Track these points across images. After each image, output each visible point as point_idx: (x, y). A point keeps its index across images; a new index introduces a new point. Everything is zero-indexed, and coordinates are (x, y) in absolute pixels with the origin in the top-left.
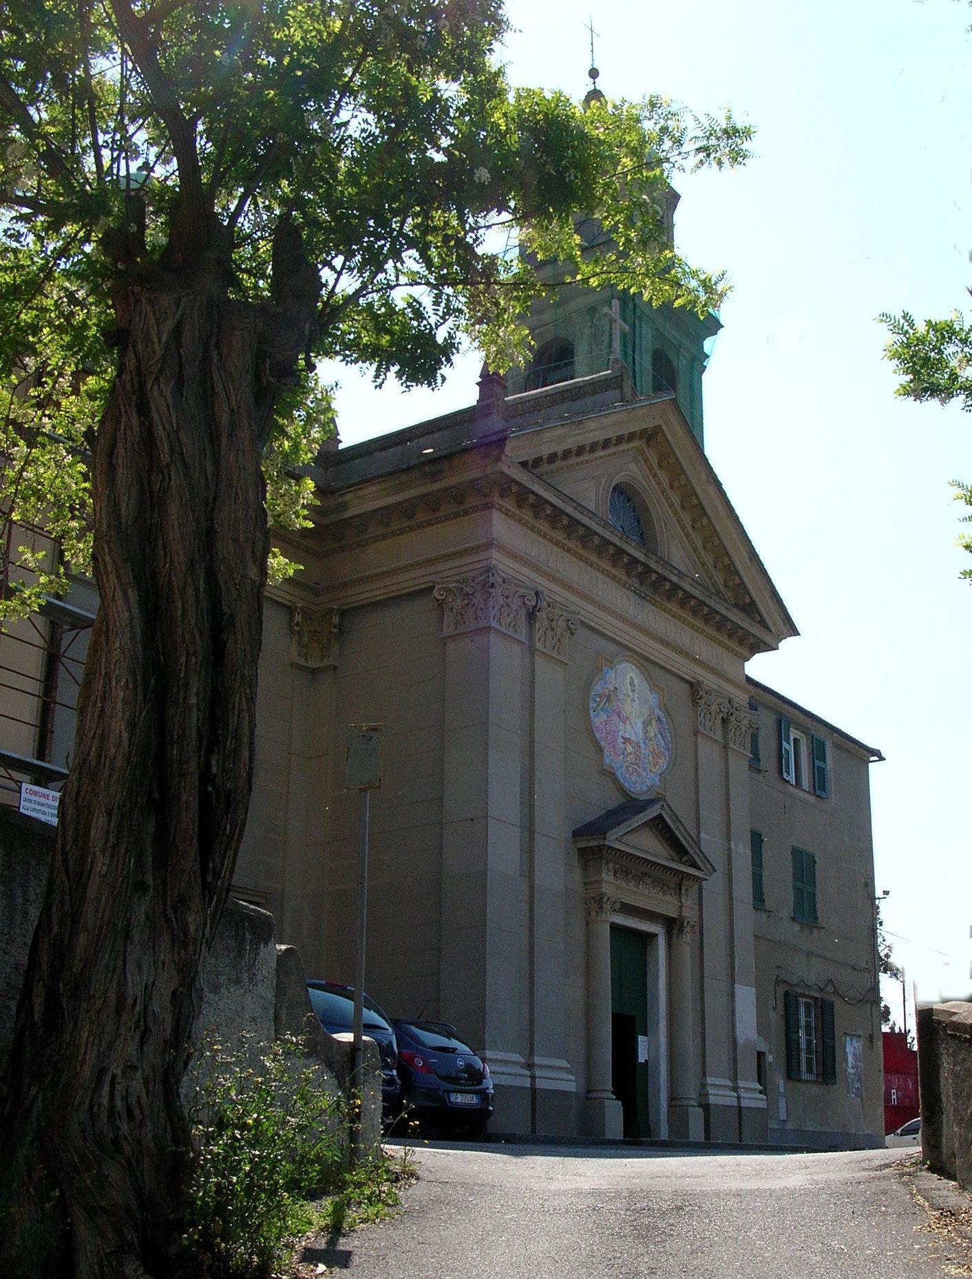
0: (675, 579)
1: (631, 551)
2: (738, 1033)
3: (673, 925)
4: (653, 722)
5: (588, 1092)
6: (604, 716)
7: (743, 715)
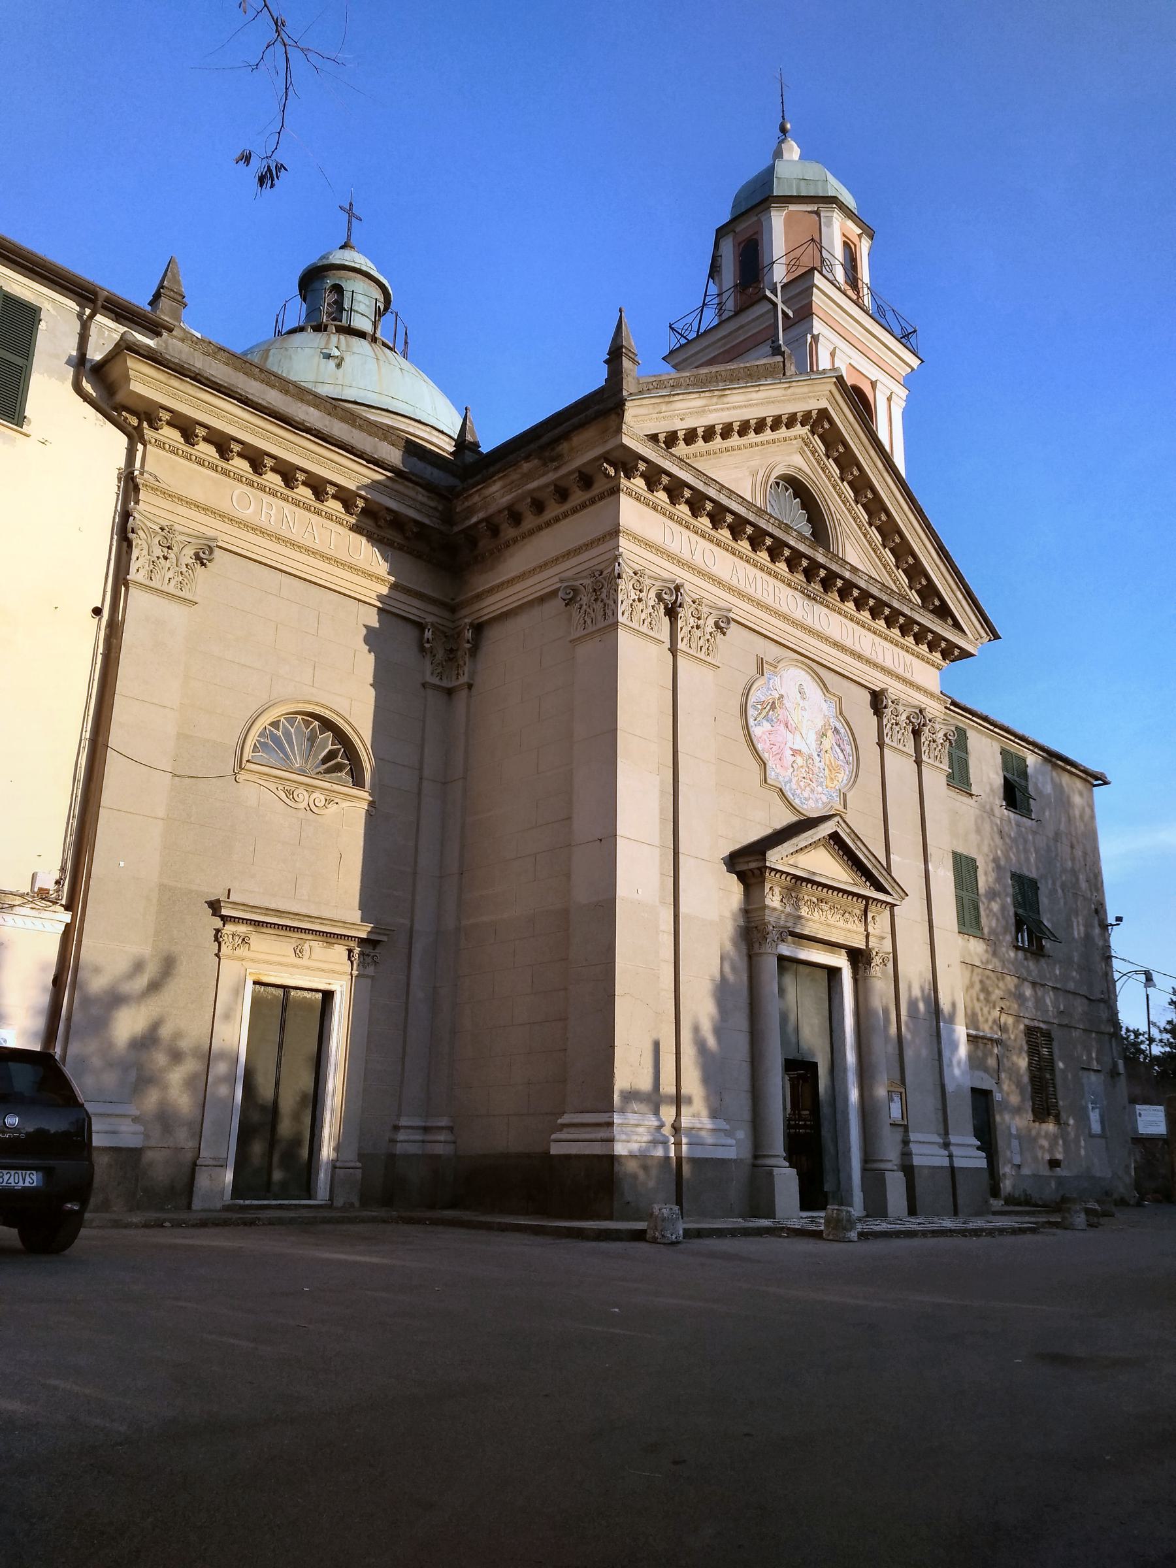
0: (847, 575)
1: (792, 543)
2: (947, 1081)
3: (859, 958)
4: (830, 733)
5: (756, 1157)
6: (767, 726)
7: (937, 726)
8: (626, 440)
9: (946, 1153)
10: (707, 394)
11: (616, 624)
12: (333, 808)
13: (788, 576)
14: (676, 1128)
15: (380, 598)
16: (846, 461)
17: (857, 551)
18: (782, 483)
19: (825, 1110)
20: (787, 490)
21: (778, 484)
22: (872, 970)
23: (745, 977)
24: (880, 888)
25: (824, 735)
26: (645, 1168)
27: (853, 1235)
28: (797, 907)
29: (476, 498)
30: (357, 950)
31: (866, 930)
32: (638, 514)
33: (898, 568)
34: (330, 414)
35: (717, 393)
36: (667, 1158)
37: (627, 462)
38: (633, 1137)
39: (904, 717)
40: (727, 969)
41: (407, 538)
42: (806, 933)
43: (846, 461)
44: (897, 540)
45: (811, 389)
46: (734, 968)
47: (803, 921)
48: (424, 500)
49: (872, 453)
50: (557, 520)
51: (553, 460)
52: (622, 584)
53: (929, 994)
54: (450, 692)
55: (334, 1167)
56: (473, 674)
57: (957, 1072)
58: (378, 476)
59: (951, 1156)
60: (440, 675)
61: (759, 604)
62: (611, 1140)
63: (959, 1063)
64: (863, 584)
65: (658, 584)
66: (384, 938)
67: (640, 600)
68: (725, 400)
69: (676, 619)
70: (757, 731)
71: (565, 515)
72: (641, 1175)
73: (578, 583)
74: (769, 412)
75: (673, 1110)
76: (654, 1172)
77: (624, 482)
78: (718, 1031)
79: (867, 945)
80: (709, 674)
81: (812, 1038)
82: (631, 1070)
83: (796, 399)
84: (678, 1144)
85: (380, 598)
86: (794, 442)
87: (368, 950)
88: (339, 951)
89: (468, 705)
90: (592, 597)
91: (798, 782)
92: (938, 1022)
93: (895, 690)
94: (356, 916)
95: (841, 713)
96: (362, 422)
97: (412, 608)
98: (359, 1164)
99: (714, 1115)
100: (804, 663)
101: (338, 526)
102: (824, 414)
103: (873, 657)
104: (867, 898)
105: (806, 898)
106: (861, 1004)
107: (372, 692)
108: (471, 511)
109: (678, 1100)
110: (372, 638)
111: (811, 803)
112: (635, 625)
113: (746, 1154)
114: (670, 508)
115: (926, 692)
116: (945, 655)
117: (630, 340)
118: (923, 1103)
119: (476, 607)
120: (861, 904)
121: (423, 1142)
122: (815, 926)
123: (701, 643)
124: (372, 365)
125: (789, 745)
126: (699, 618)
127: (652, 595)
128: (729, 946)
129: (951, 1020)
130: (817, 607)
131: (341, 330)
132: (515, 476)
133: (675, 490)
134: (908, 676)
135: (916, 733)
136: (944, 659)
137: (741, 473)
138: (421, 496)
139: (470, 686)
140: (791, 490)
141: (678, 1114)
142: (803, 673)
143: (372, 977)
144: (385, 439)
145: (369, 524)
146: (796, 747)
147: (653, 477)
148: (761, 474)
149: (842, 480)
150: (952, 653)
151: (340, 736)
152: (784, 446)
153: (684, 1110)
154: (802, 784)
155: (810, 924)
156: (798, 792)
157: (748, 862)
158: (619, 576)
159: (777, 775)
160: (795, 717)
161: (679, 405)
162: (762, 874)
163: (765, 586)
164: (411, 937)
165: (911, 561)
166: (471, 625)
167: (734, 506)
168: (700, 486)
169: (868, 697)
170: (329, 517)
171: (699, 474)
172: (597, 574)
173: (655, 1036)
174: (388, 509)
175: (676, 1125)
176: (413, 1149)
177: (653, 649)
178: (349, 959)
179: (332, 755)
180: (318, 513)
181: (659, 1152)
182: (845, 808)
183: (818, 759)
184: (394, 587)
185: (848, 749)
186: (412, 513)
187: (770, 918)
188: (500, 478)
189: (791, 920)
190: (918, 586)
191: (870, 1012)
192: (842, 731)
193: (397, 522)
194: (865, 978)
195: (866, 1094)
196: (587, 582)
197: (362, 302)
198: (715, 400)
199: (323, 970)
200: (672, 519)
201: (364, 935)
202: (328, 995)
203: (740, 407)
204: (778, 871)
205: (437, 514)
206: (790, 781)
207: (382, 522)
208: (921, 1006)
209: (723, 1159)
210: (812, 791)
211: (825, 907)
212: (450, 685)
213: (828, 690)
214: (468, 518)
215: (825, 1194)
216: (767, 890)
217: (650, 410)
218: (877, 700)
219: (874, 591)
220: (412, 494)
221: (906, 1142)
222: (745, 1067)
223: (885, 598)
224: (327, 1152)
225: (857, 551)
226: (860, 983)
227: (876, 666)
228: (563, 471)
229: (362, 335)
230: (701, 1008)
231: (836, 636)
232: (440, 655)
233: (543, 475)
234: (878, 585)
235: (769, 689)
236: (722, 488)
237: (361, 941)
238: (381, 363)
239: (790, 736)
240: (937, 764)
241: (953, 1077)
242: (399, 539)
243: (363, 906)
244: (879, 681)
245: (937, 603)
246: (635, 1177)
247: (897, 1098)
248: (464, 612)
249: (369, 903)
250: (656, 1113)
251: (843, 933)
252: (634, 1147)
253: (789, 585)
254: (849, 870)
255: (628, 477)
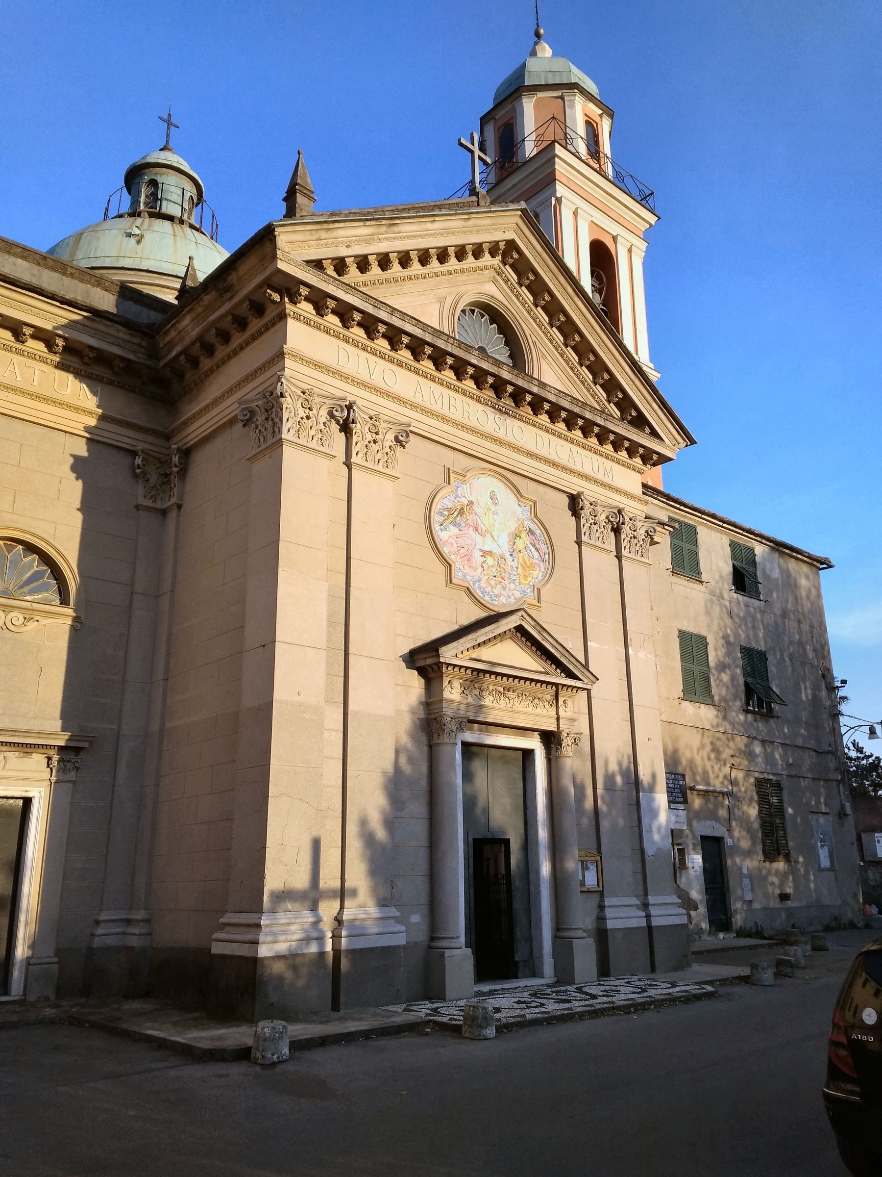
0: (535, 390)
1: (474, 361)
2: (646, 846)
3: (550, 739)
4: (524, 535)
5: (432, 939)
6: (454, 530)
7: (638, 524)
8: (281, 265)
9: (644, 914)
10: (373, 223)
11: (280, 442)
12: (32, 625)
13: (477, 392)
14: (339, 920)
15: (87, 429)
16: (538, 288)
17: (552, 370)
18: (477, 310)
19: (517, 883)
20: (483, 316)
21: (473, 311)
22: (563, 750)
23: (424, 769)
24: (571, 675)
25: (518, 536)
26: (295, 968)
27: (491, 1032)
28: (480, 697)
29: (173, 333)
30: (56, 758)
31: (557, 714)
32: (306, 338)
33: (595, 384)
34: (39, 264)
35: (384, 222)
36: (322, 954)
37: (290, 288)
38: (281, 937)
39: (603, 517)
40: (403, 760)
41: (116, 374)
42: (489, 720)
43: (538, 288)
44: (592, 358)
45: (494, 221)
46: (411, 760)
47: (485, 710)
48: (126, 337)
49: (562, 280)
50: (241, 348)
51: (227, 290)
52: (287, 402)
53: (628, 768)
54: (164, 513)
55: (29, 964)
56: (181, 497)
57: (656, 837)
58: (75, 316)
59: (648, 917)
60: (154, 498)
61: (444, 419)
62: (256, 943)
63: (659, 829)
64: (552, 398)
65: (328, 402)
66: (86, 745)
67: (308, 418)
68: (396, 229)
69: (351, 435)
70: (443, 535)
71: (248, 344)
72: (289, 975)
73: (254, 405)
74: (451, 241)
75: (337, 904)
76: (304, 971)
77: (289, 307)
78: (389, 823)
79: (558, 728)
80: (388, 486)
81: (503, 816)
82: (284, 868)
83: (479, 230)
84: (336, 937)
85: (87, 429)
86: (486, 272)
87: (71, 757)
88: (38, 760)
89: (178, 523)
90: (263, 418)
91: (488, 581)
92: (638, 792)
93: (590, 492)
94: (57, 724)
95: (536, 516)
96: (73, 271)
97: (125, 438)
98: (56, 960)
99: (382, 903)
100: (495, 472)
101: (42, 364)
102: (511, 245)
103: (571, 465)
104: (556, 685)
105: (491, 688)
106: (553, 784)
107: (79, 516)
108: (171, 345)
109: (343, 894)
110: (79, 466)
111: (503, 599)
112: (302, 441)
113: (421, 936)
114: (343, 331)
115: (625, 494)
116: (645, 459)
117: (307, 179)
118: (621, 869)
119: (184, 434)
120: (552, 690)
121: (124, 934)
122: (500, 713)
123: (379, 456)
124: (169, 240)
125: (478, 547)
126: (377, 433)
127: (324, 412)
128: (405, 740)
129: (652, 789)
130: (509, 420)
131: (152, 215)
132: (199, 309)
133: (344, 312)
134: (607, 480)
135: (617, 531)
136: (645, 464)
137: (427, 302)
138: (123, 334)
139: (179, 507)
140: (487, 317)
141: (342, 907)
142: (495, 480)
143: (74, 783)
144: (98, 285)
145: (74, 361)
146: (486, 548)
147: (319, 300)
148: (449, 301)
149: (536, 306)
150: (650, 458)
151: (46, 559)
152: (474, 276)
153: (347, 903)
154: (493, 582)
155: (494, 712)
156: (488, 589)
157: (425, 659)
158: (282, 395)
159: (465, 575)
160: (485, 522)
161: (341, 233)
162: (440, 668)
163: (453, 402)
164: (118, 738)
165: (606, 376)
166: (178, 450)
167: (408, 328)
168: (370, 309)
169: (566, 500)
170: (32, 356)
171: (368, 297)
172: (268, 394)
173: (315, 834)
174: (91, 348)
175: (339, 918)
176: (111, 941)
177: (324, 463)
178: (48, 766)
179: (36, 576)
180: (19, 353)
181: (313, 948)
182: (539, 601)
183: (511, 558)
184: (102, 418)
185: (544, 548)
186: (114, 350)
187: (448, 711)
188: (188, 312)
189: (471, 709)
190: (616, 400)
191: (563, 792)
192: (538, 532)
193: (101, 358)
194: (557, 758)
195: (558, 866)
196: (260, 403)
197: (175, 193)
198: (384, 229)
199: (18, 779)
200: (347, 342)
201: (62, 743)
202: (28, 801)
203: (415, 237)
204: (455, 666)
205: (143, 350)
206: (479, 580)
207: (86, 360)
208: (619, 780)
209: (390, 947)
210: (504, 588)
211: (511, 694)
212: (164, 506)
213: (521, 496)
214: (169, 352)
215: (516, 964)
216: (445, 683)
217: (307, 236)
218: (575, 503)
219: (566, 404)
220: (113, 332)
221: (602, 907)
222: (423, 853)
223: (577, 410)
224: (21, 951)
225: (552, 370)
226: (553, 762)
227: (572, 472)
228: (235, 300)
229: (170, 218)
230: (371, 801)
231: (531, 447)
232: (154, 479)
233: (220, 307)
234: (569, 399)
235: (457, 496)
236: (393, 310)
237: (61, 749)
238: (178, 238)
239: (479, 539)
240: (638, 557)
241: (653, 842)
242: (107, 374)
243: (65, 715)
244: (575, 485)
245: (634, 414)
246: (281, 978)
247: (593, 867)
248: (176, 439)
249: (67, 715)
250: (314, 908)
251: (532, 718)
252: (282, 947)
253: (479, 401)
254: (538, 659)
255: (294, 303)
